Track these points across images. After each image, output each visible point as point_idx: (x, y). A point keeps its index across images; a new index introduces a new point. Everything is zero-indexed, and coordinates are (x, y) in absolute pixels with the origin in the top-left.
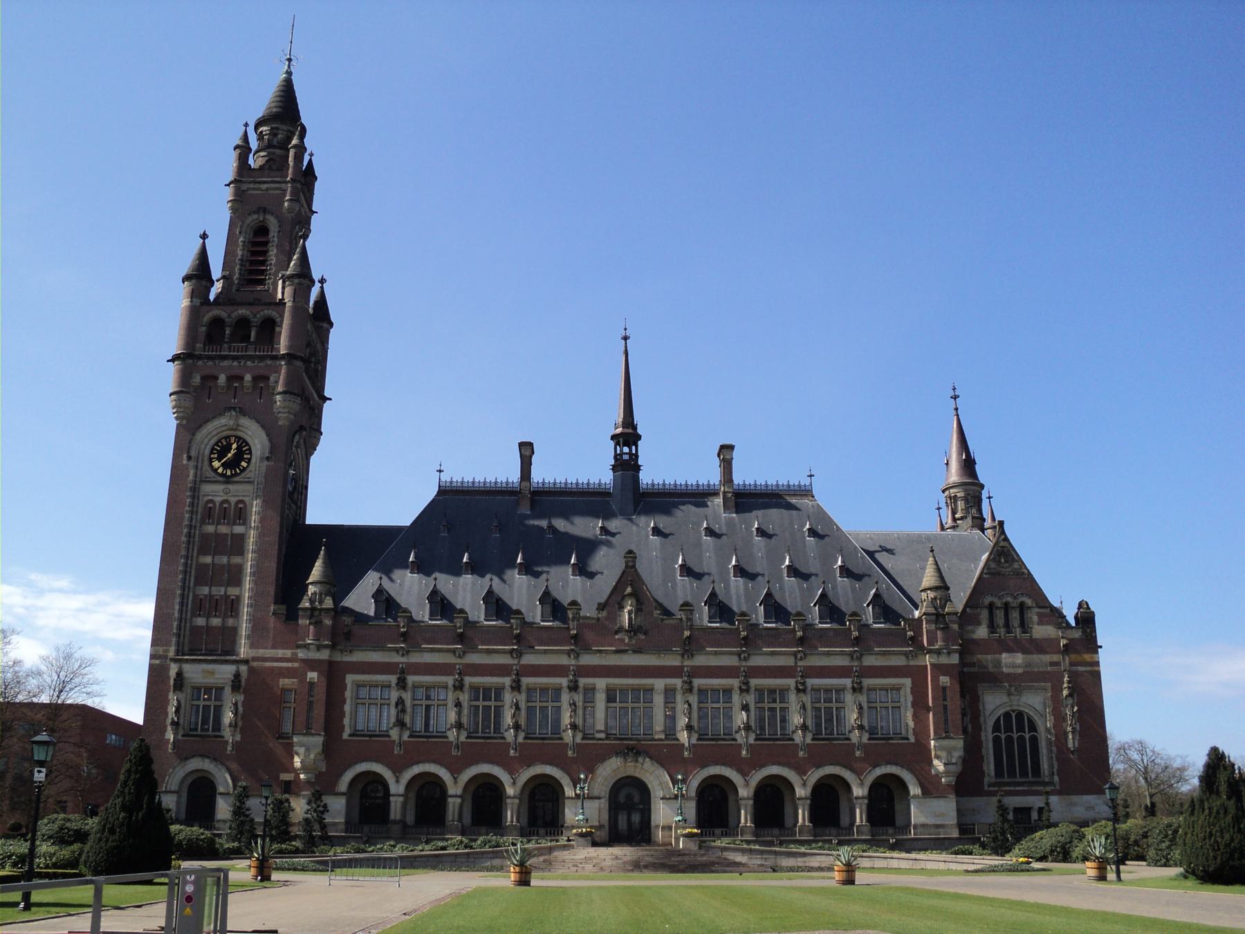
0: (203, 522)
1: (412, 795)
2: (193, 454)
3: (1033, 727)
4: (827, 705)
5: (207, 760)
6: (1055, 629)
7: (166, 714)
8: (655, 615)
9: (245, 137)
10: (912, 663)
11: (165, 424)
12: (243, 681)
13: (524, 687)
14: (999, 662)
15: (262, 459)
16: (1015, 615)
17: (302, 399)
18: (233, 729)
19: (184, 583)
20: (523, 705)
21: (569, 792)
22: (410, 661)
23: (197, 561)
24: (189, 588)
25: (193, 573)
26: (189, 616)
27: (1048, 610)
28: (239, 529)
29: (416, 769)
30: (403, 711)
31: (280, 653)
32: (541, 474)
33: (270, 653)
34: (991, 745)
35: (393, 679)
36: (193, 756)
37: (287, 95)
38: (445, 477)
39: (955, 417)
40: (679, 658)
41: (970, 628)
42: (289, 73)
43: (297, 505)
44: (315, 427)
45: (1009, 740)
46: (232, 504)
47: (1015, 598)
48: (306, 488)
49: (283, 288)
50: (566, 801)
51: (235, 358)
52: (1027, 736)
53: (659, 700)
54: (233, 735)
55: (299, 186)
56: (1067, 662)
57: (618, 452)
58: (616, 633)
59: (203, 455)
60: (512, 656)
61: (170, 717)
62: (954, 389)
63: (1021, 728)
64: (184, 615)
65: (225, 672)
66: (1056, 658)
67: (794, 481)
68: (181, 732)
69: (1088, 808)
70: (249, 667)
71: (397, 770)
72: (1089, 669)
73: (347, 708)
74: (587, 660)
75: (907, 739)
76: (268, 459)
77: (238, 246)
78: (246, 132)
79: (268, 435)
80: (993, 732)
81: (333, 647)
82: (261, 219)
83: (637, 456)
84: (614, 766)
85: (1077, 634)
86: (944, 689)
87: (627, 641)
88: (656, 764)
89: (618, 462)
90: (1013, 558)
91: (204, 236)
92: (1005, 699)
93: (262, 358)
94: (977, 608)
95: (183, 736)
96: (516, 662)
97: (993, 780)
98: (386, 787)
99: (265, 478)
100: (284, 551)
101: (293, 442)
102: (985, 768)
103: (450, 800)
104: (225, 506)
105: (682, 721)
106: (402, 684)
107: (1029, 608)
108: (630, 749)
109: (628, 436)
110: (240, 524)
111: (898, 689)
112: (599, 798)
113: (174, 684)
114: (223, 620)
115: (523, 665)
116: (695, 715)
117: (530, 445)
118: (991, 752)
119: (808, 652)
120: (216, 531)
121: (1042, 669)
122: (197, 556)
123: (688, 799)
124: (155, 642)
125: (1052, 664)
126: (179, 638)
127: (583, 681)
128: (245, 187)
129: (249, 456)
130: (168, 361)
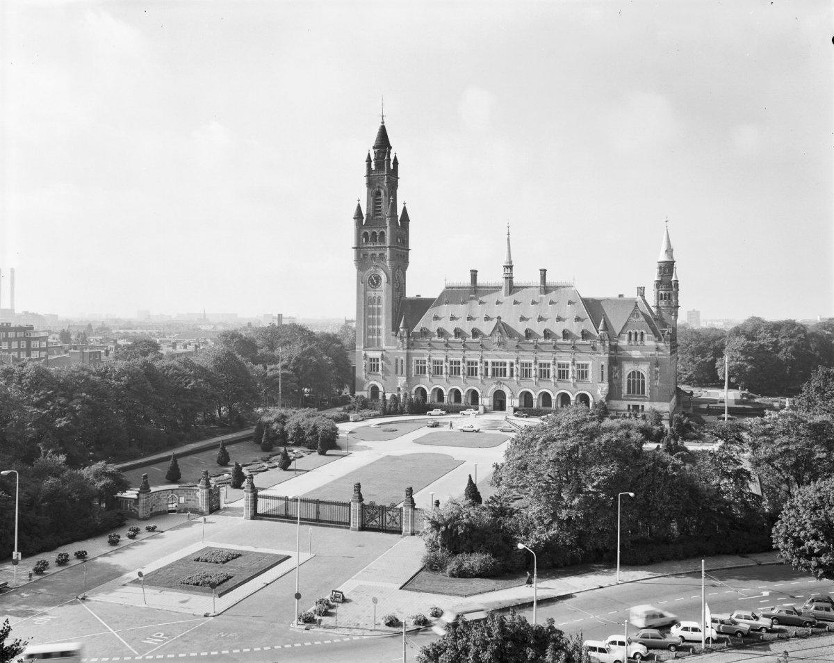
3: (643, 377)
11: (353, 270)
16: (639, 337)
21: (480, 394)
33: (390, 347)
34: (626, 385)
37: (383, 135)
42: (383, 123)
45: (634, 381)
48: (405, 284)
73: (413, 367)
91: (359, 201)
105: (515, 373)
125: (651, 355)
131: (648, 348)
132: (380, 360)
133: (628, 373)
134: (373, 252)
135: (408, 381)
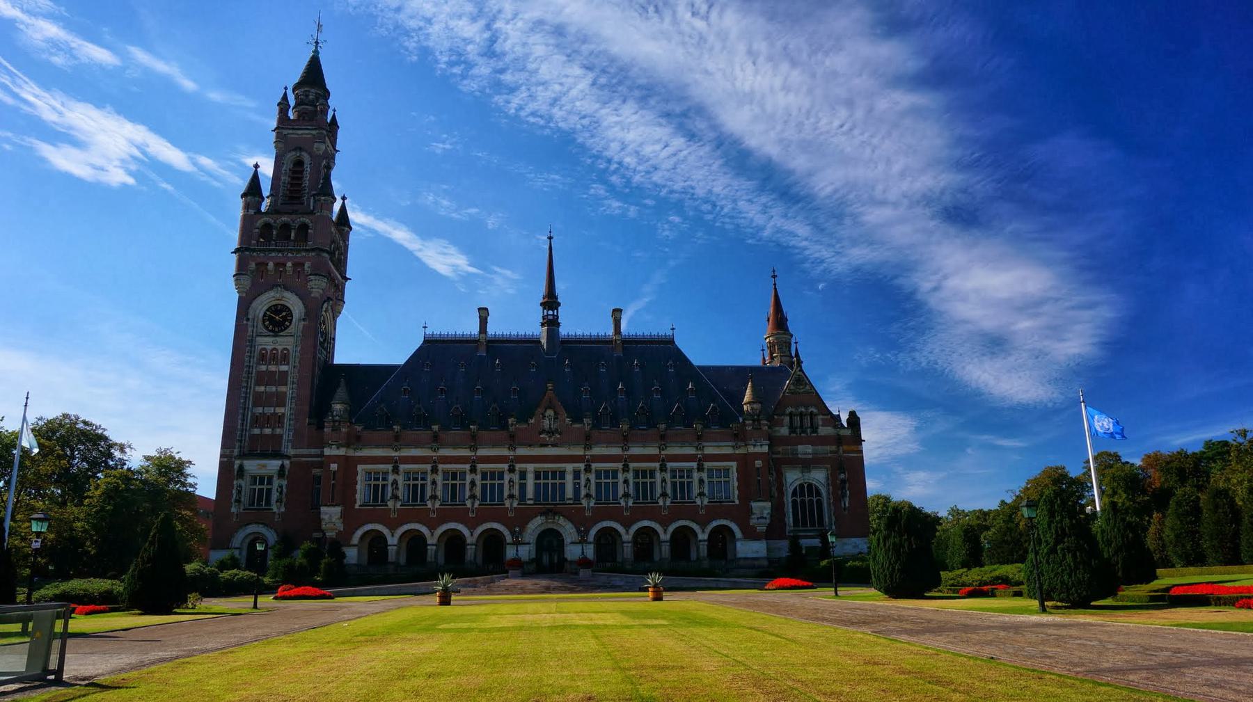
0: (258, 364)
1: (404, 545)
2: (250, 317)
3: (818, 493)
4: (681, 480)
5: (261, 526)
6: (833, 430)
7: (232, 495)
8: (567, 422)
9: (285, 97)
10: (737, 452)
12: (287, 471)
13: (479, 471)
14: (797, 450)
15: (300, 320)
16: (807, 421)
17: (328, 279)
18: (278, 504)
19: (245, 405)
20: (478, 483)
21: (509, 539)
22: (402, 454)
23: (254, 390)
24: (248, 408)
25: (251, 398)
26: (248, 428)
27: (829, 417)
28: (284, 368)
29: (406, 527)
30: (397, 488)
31: (313, 451)
32: (494, 329)
34: (790, 505)
35: (390, 467)
36: (251, 524)
38: (429, 331)
39: (773, 291)
40: (583, 450)
41: (777, 428)
42: (316, 52)
43: (327, 351)
44: (340, 298)
45: (803, 502)
46: (279, 351)
47: (806, 407)
49: (315, 201)
50: (508, 546)
51: (279, 251)
52: (815, 500)
53: (569, 478)
54: (279, 509)
55: (324, 132)
56: (841, 451)
57: (545, 314)
58: (541, 433)
59: (258, 317)
60: (471, 450)
61: (234, 497)
62: (774, 271)
63: (810, 494)
64: (244, 427)
65: (273, 465)
66: (834, 448)
67: (662, 333)
68: (242, 508)
69: (854, 547)
70: (291, 463)
71: (393, 529)
72: (855, 455)
73: (358, 487)
74: (522, 451)
75: (734, 502)
76: (304, 320)
77: (282, 173)
78: (285, 94)
79: (304, 304)
80: (792, 497)
81: (348, 446)
82: (298, 155)
83: (557, 316)
84: (540, 522)
85: (848, 432)
86: (758, 469)
87: (547, 439)
88: (566, 520)
89: (545, 321)
90: (806, 384)
92: (800, 475)
93: (299, 251)
94: (782, 415)
95: (244, 510)
96: (473, 454)
97: (792, 528)
98: (385, 539)
99: (302, 333)
100: (316, 382)
101: (322, 308)
102: (786, 519)
103: (429, 547)
104: (275, 352)
105: (583, 492)
106: (396, 470)
107: (816, 415)
108: (550, 510)
109: (551, 302)
110: (284, 364)
111: (728, 470)
112: (529, 544)
113: (237, 475)
114: (273, 430)
115: (477, 456)
116: (593, 487)
117: (486, 309)
118: (791, 510)
119: (668, 445)
120: (267, 369)
121: (824, 456)
122: (254, 388)
123: (590, 543)
124: (224, 446)
125: (831, 452)
126: (241, 443)
127: (518, 466)
128: (285, 132)
129: (290, 318)
130: (232, 253)
131: (824, 440)
132: (275, 479)
133: (793, 488)
134: (281, 261)
135: (344, 516)
